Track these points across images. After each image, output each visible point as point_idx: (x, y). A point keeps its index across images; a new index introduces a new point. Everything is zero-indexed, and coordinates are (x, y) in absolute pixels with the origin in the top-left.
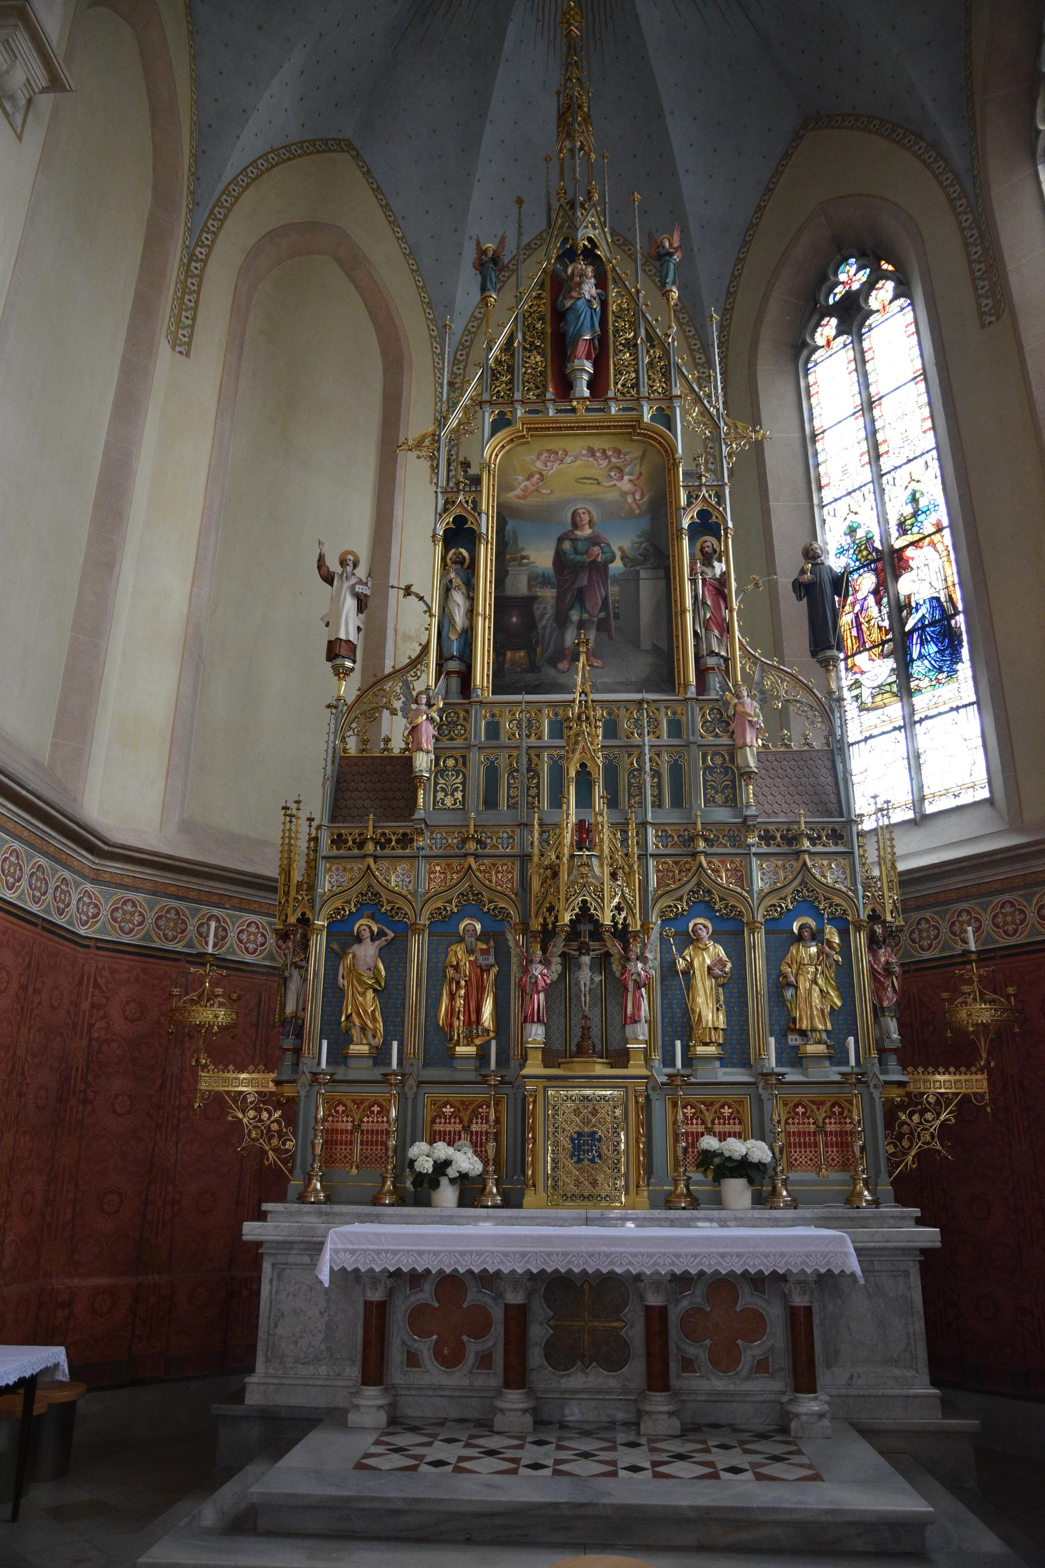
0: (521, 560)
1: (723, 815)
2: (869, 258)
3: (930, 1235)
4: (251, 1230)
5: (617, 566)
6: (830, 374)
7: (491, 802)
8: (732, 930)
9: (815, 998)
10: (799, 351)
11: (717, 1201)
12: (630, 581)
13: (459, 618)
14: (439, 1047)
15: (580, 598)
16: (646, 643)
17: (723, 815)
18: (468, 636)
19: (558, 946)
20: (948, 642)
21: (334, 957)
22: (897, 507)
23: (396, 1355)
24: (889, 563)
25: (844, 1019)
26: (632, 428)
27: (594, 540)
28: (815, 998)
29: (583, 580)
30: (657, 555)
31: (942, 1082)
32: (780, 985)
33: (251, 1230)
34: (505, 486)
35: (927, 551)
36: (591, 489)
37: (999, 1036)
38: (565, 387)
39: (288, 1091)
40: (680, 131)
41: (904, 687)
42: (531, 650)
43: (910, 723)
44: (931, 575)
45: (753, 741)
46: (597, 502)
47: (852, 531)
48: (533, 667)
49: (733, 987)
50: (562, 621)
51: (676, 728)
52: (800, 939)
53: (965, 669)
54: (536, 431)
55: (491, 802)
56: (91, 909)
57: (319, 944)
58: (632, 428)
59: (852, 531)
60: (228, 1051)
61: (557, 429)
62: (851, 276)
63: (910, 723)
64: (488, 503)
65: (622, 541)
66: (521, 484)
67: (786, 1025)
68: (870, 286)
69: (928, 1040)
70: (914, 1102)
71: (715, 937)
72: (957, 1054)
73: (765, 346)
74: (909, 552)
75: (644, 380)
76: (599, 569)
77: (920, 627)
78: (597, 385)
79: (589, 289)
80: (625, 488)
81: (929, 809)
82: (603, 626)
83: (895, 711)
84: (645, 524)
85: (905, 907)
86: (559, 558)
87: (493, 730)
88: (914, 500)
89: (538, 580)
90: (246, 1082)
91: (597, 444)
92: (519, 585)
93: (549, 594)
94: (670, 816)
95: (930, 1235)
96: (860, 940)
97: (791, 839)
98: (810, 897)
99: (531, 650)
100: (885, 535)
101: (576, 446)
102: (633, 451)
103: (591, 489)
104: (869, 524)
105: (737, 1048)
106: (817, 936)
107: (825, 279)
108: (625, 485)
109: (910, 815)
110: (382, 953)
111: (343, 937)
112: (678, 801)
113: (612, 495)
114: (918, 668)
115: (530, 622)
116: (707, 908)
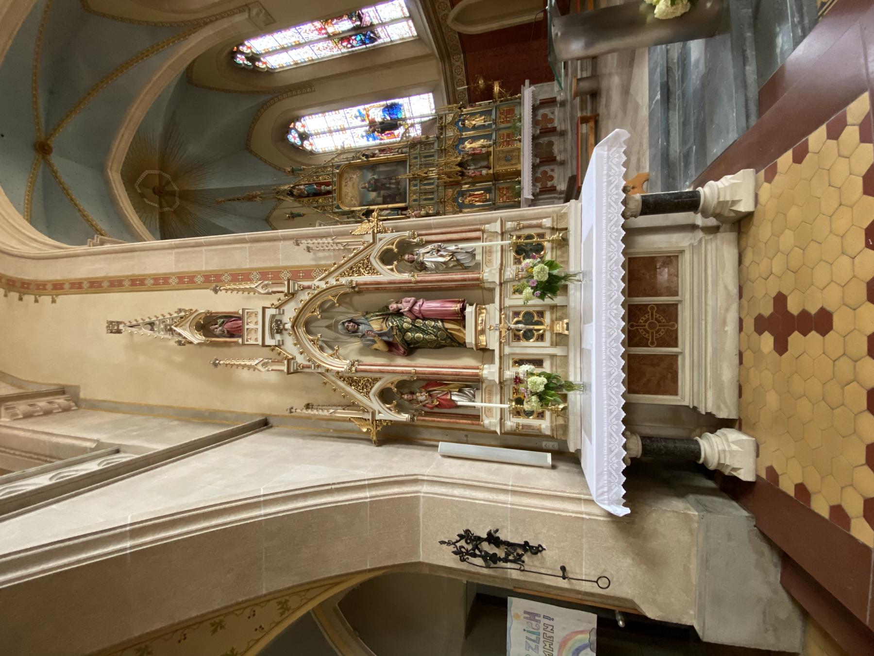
0: (373, 200)
1: (436, 145)
3: (527, 82)
5: (375, 177)
8: (462, 140)
9: (478, 121)
12: (380, 173)
13: (388, 212)
15: (384, 185)
16: (394, 168)
17: (436, 145)
22: (358, 122)
25: (481, 114)
26: (340, 175)
27: (369, 182)
29: (379, 184)
30: (373, 167)
32: (474, 128)
34: (355, 206)
35: (370, 113)
36: (355, 185)
37: (486, 79)
38: (329, 192)
42: (396, 195)
44: (376, 111)
46: (359, 183)
47: (363, 137)
48: (400, 194)
49: (474, 139)
50: (389, 188)
51: (416, 158)
52: (464, 125)
54: (340, 198)
58: (340, 175)
59: (363, 137)
61: (340, 194)
64: (359, 208)
65: (370, 176)
66: (354, 202)
69: (488, 94)
71: (463, 144)
72: (490, 89)
76: (376, 181)
77: (389, 114)
78: (327, 184)
79: (302, 187)
80: (355, 177)
82: (391, 179)
84: (365, 171)
85: (456, 102)
86: (373, 191)
87: (415, 200)
88: (356, 117)
89: (379, 196)
91: (344, 184)
92: (380, 199)
93: (382, 192)
94: (436, 157)
95: (527, 82)
97: (442, 129)
98: (454, 123)
99: (396, 195)
101: (344, 189)
102: (346, 175)
103: (355, 185)
104: (362, 131)
105: (487, 137)
106: (464, 121)
107: (293, 146)
108: (355, 177)
112: (433, 156)
113: (358, 180)
115: (389, 196)
116: (457, 146)
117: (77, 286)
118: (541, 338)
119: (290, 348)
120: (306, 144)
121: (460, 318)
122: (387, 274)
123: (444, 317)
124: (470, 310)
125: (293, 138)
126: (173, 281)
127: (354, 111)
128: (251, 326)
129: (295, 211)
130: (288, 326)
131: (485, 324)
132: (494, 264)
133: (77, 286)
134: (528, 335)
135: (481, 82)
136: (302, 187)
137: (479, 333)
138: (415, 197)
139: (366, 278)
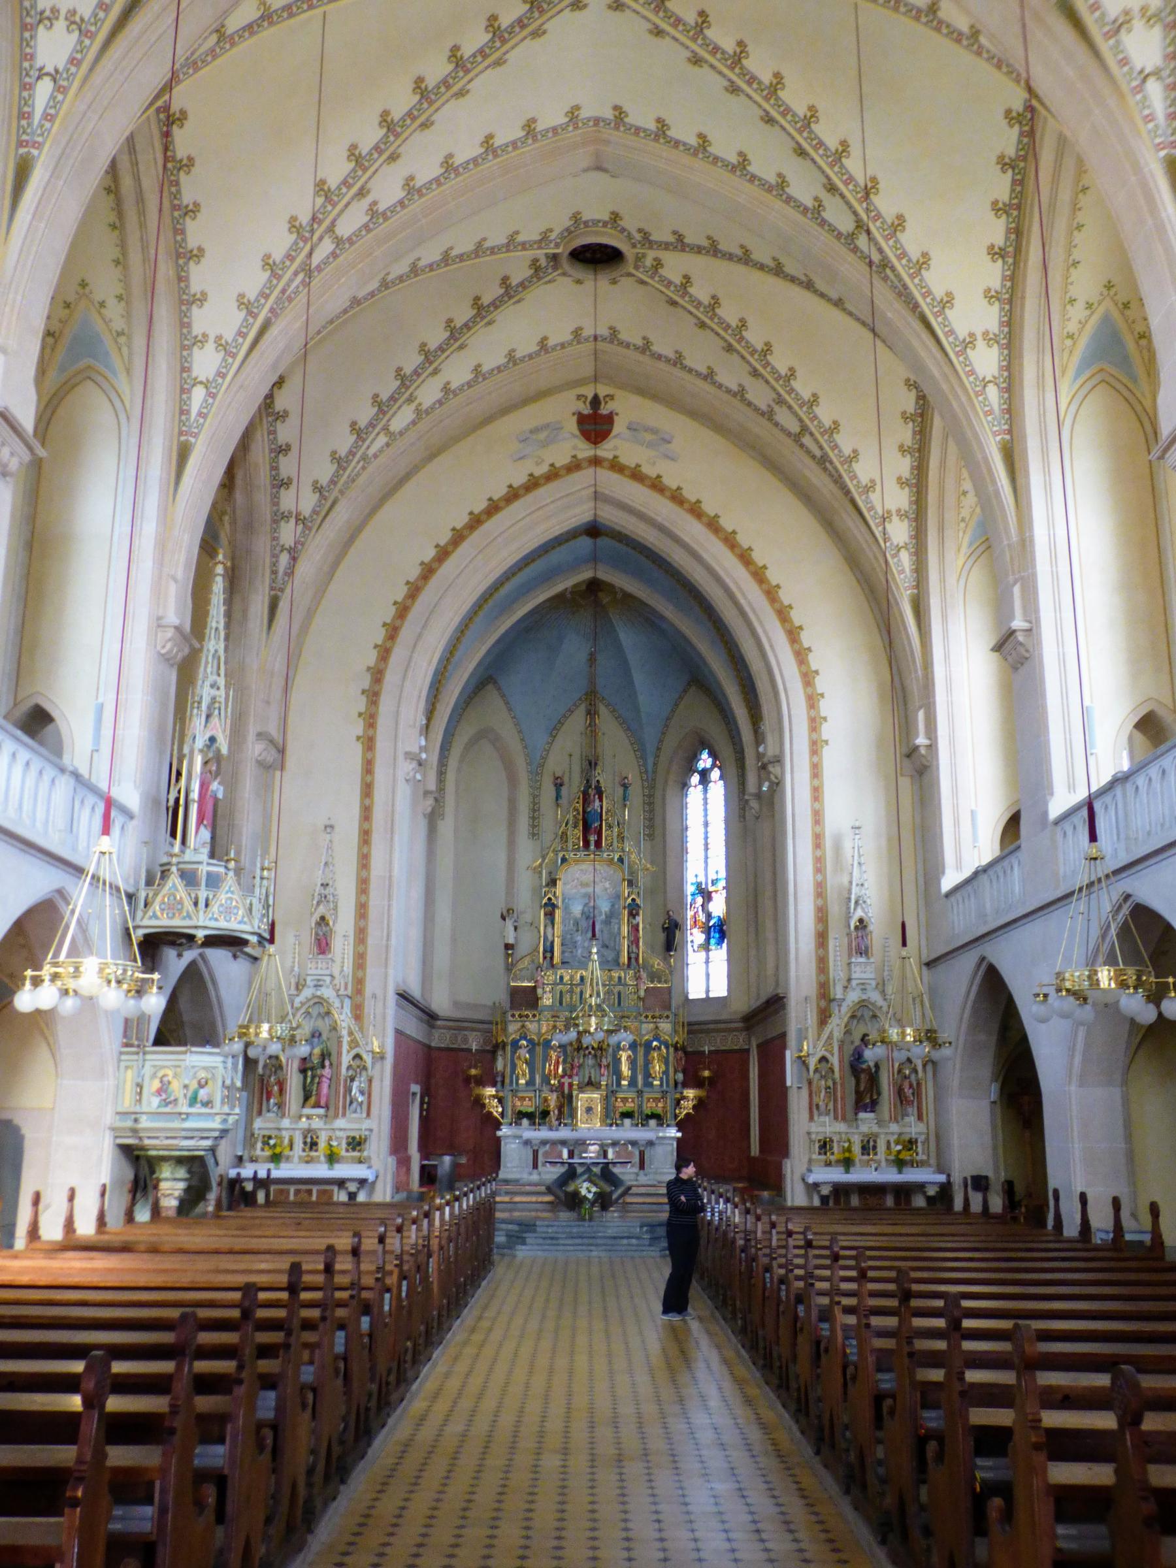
2: (713, 754)
3: (679, 1135)
4: (499, 1133)
6: (694, 794)
7: (561, 1003)
9: (657, 1067)
10: (685, 785)
11: (622, 1125)
14: (546, 1080)
18: (552, 943)
19: (582, 1052)
20: (722, 936)
21: (513, 1053)
22: (712, 876)
23: (540, 1164)
24: (707, 896)
25: (666, 1072)
28: (657, 1067)
31: (690, 1093)
33: (499, 1133)
39: (501, 1094)
40: (638, 678)
41: (706, 947)
43: (707, 962)
44: (718, 907)
45: (643, 987)
49: (633, 1063)
53: (725, 945)
55: (561, 1003)
56: (440, 1039)
57: (509, 1048)
60: (481, 1082)
62: (705, 761)
63: (707, 962)
67: (648, 1075)
68: (712, 769)
70: (684, 1098)
73: (670, 783)
74: (713, 895)
75: (615, 843)
77: (714, 925)
81: (711, 995)
83: (703, 954)
87: (561, 978)
90: (490, 1091)
95: (679, 1135)
96: (671, 1050)
100: (706, 884)
107: (695, 757)
109: (704, 996)
110: (529, 1052)
111: (515, 1045)
114: (713, 941)
117: (368, 767)
118: (304, 1150)
119: (307, 993)
120: (695, 779)
121: (317, 1105)
122: (346, 1059)
123: (318, 1095)
124: (321, 1111)
125: (705, 761)
126: (364, 874)
127: (723, 874)
128: (320, 965)
129: (564, 791)
130: (319, 993)
131: (314, 1119)
132: (345, 1125)
133: (368, 767)
134: (305, 1143)
135: (706, 1073)
136: (597, 803)
137: (309, 1117)
138: (566, 978)
139: (345, 1047)
